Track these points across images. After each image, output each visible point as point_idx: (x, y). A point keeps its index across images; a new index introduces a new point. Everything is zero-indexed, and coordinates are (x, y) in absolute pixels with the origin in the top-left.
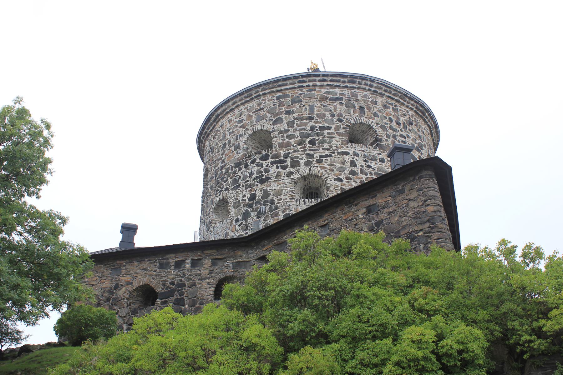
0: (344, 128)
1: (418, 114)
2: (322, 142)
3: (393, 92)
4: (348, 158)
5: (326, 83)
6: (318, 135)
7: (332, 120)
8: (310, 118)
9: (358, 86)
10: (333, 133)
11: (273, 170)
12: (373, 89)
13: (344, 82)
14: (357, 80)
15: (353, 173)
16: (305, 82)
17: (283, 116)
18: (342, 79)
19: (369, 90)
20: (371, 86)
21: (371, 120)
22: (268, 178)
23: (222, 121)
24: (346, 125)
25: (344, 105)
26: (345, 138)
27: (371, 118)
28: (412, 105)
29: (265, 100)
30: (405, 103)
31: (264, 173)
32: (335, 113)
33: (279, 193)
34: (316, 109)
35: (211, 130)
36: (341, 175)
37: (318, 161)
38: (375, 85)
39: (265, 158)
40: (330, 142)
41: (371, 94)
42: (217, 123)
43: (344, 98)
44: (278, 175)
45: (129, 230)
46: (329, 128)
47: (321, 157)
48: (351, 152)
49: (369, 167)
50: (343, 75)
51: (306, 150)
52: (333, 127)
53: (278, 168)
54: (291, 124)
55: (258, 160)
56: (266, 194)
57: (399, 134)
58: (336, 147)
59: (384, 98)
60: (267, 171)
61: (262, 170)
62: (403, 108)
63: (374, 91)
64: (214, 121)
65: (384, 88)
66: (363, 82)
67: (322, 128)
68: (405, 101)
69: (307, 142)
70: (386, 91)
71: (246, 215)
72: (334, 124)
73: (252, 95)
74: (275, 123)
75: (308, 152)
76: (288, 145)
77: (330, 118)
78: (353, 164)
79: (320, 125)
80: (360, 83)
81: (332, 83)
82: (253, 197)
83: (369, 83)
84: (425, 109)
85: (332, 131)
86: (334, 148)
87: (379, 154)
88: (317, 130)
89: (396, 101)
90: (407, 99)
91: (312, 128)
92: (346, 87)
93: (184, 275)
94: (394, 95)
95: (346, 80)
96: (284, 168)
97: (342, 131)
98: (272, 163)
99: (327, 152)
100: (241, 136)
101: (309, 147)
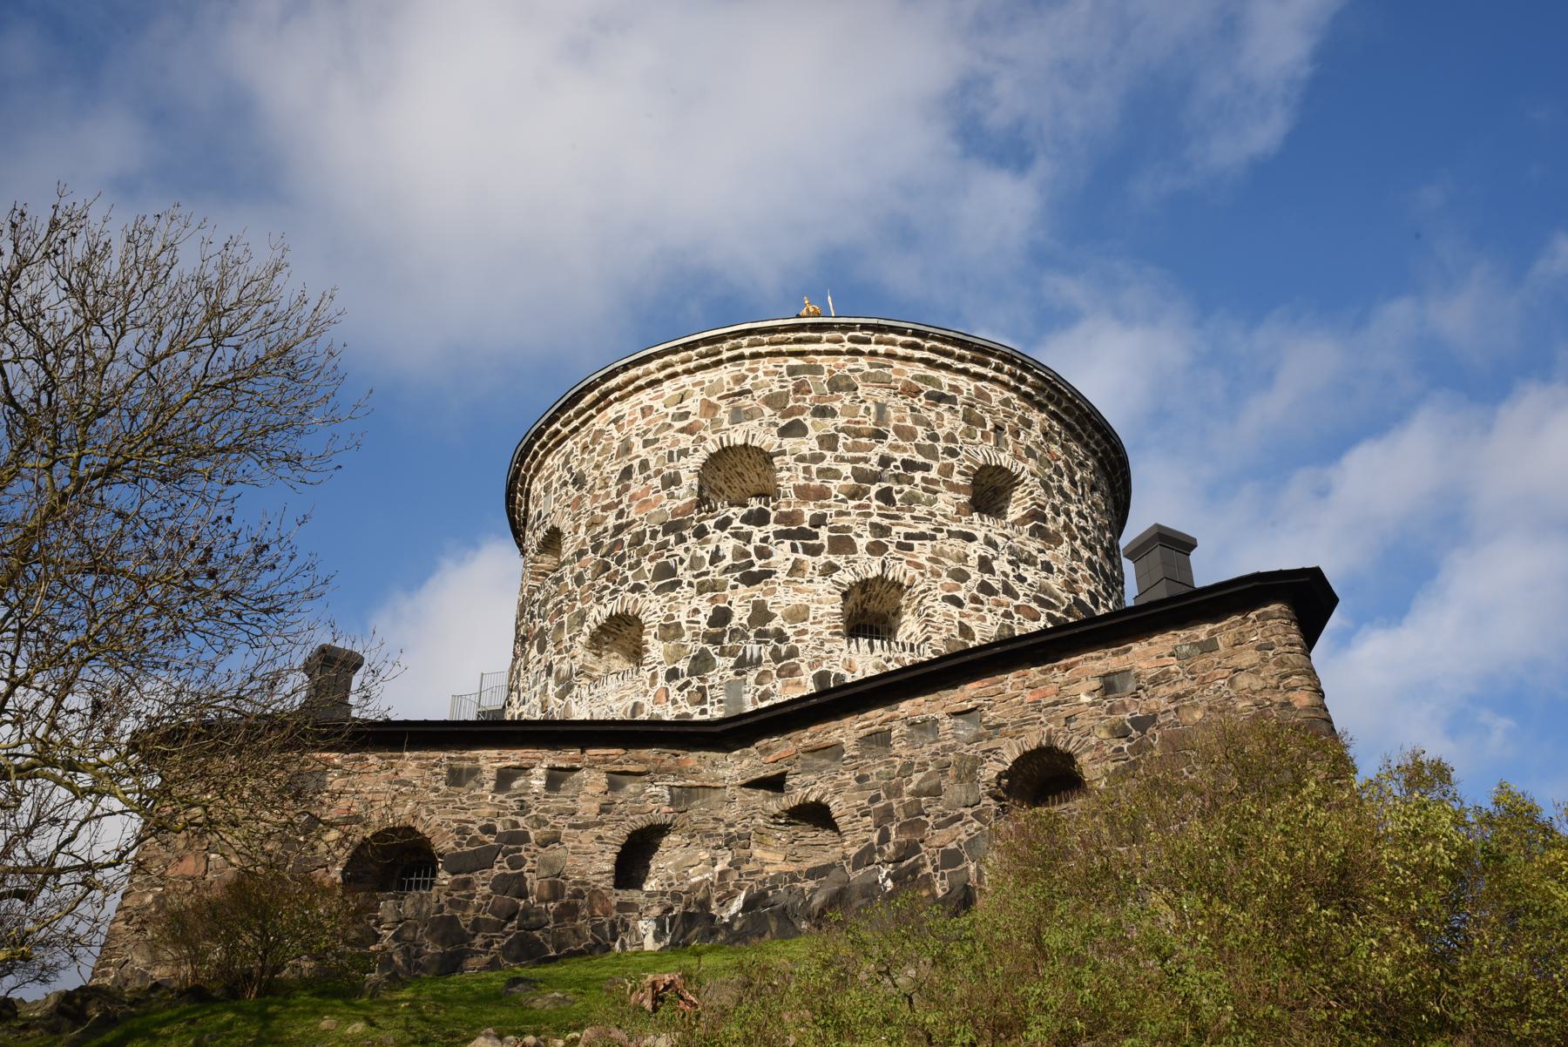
0: (960, 473)
2: (911, 499)
5: (918, 354)
6: (898, 479)
7: (934, 449)
8: (880, 435)
10: (934, 482)
11: (782, 555)
13: (961, 359)
15: (985, 588)
16: (868, 342)
17: (808, 420)
18: (957, 351)
21: (1021, 465)
22: (767, 574)
23: (616, 406)
24: (967, 467)
25: (961, 415)
26: (964, 499)
27: (1021, 459)
28: (1097, 443)
29: (756, 370)
31: (754, 558)
32: (940, 432)
33: (798, 615)
35: (576, 429)
36: (959, 588)
37: (900, 546)
38: (1030, 378)
39: (760, 518)
40: (931, 503)
42: (599, 411)
43: (960, 399)
44: (796, 568)
47: (908, 536)
48: (980, 535)
49: (1022, 579)
51: (870, 515)
52: (936, 465)
53: (794, 549)
54: (829, 442)
55: (736, 523)
56: (761, 614)
58: (945, 516)
60: (763, 553)
61: (750, 548)
64: (591, 406)
66: (1007, 367)
67: (909, 465)
69: (872, 494)
71: (701, 663)
72: (937, 459)
73: (720, 353)
74: (784, 432)
75: (876, 519)
76: (822, 494)
77: (928, 442)
78: (985, 565)
79: (906, 456)
80: (998, 369)
81: (933, 356)
82: (721, 617)
85: (933, 474)
86: (940, 518)
87: (1040, 551)
88: (897, 467)
91: (885, 461)
92: (965, 372)
93: (523, 808)
94: (1065, 410)
96: (814, 551)
97: (956, 479)
98: (779, 535)
99: (923, 527)
100: (684, 453)
101: (879, 508)
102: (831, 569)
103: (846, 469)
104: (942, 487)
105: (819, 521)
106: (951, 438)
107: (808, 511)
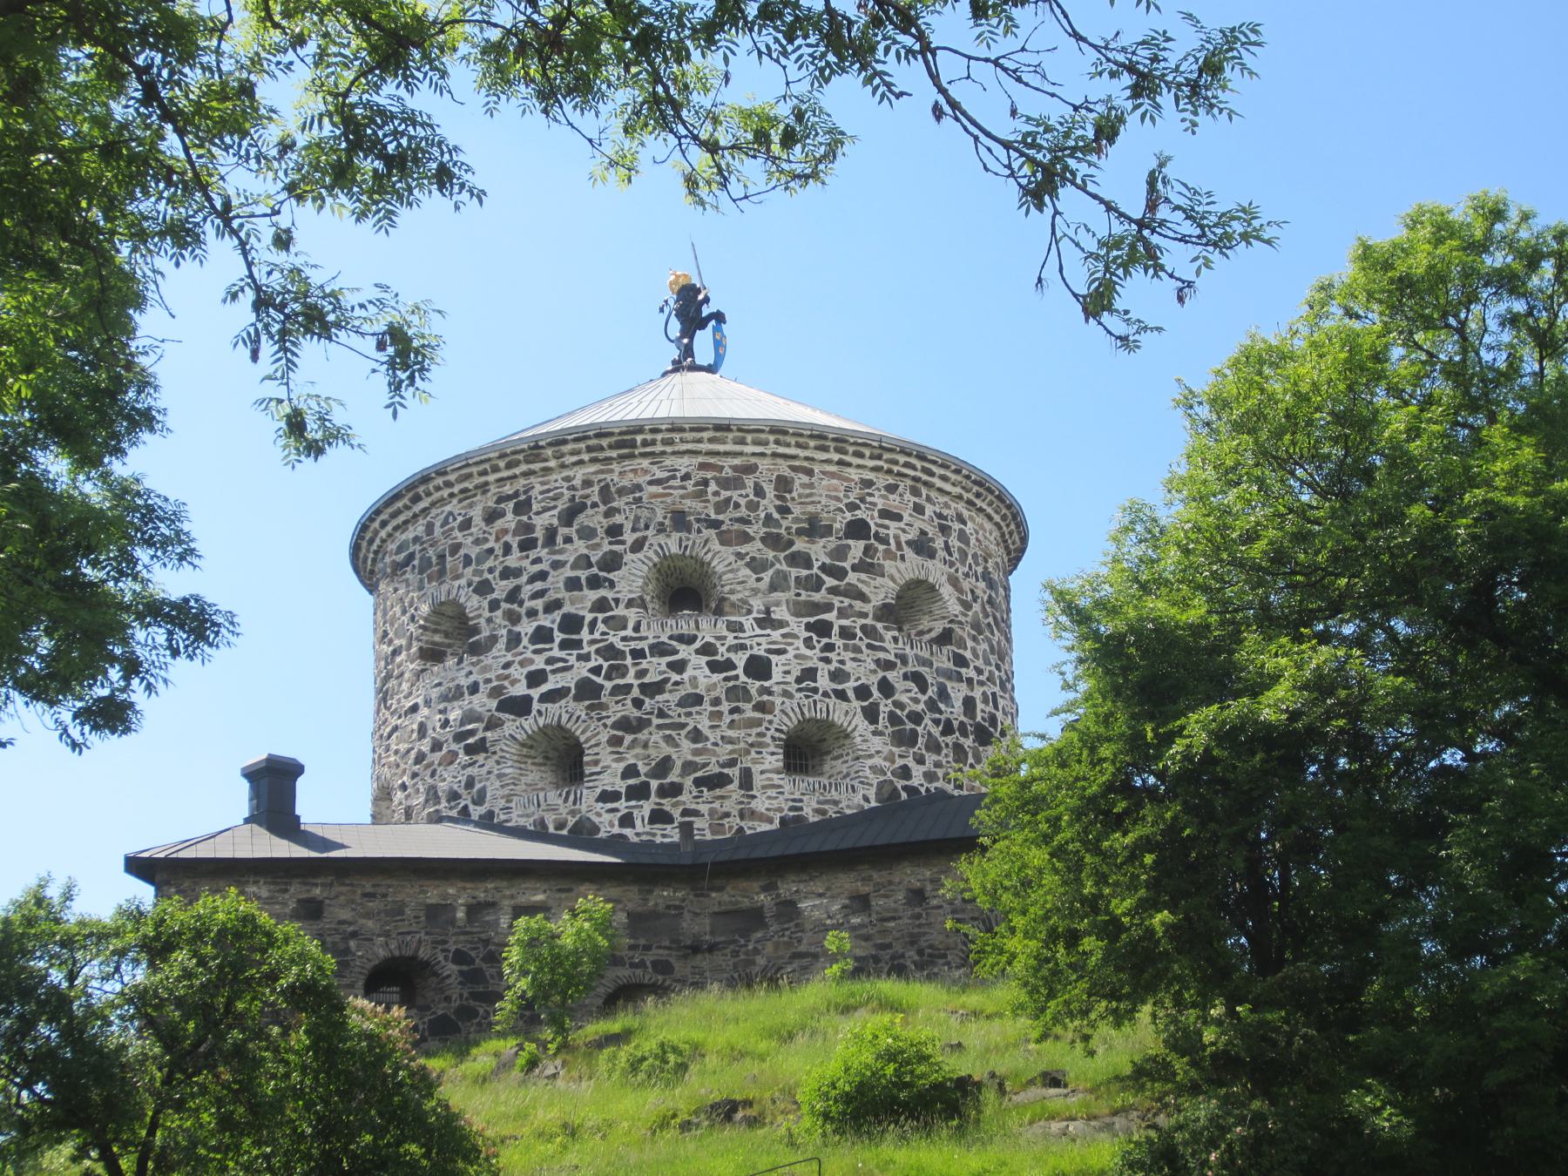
1: (609, 460)
3: (502, 464)
9: (429, 500)
12: (456, 490)
13: (407, 508)
14: (421, 490)
18: (400, 504)
19: (452, 495)
20: (448, 484)
28: (573, 453)
30: (552, 464)
38: (452, 478)
41: (460, 501)
50: (395, 497)
57: (524, 578)
59: (493, 489)
62: (554, 477)
63: (463, 491)
65: (475, 470)
68: (546, 460)
70: (484, 473)
80: (428, 494)
83: (440, 481)
84: (621, 434)
89: (526, 474)
90: (549, 452)
94: (509, 466)
95: (406, 501)
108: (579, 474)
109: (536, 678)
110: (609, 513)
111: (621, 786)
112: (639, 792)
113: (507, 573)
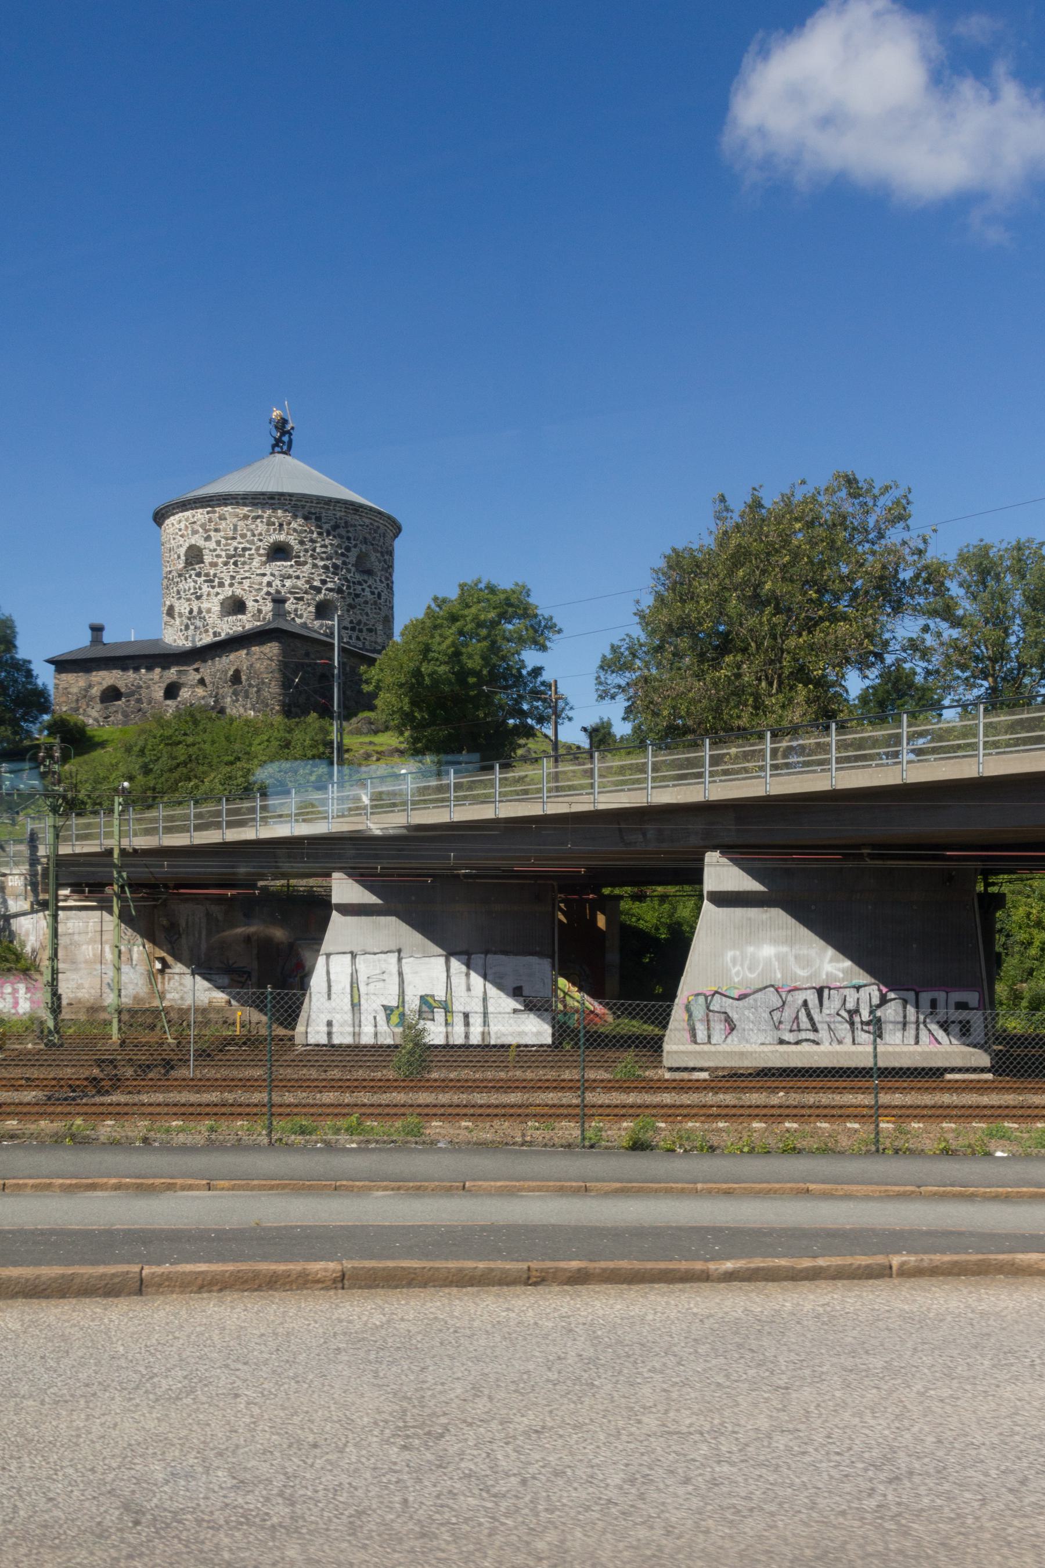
2: (244, 563)
4: (266, 579)
6: (240, 556)
8: (234, 538)
11: (205, 588)
17: (212, 534)
26: (264, 559)
33: (209, 611)
34: (239, 528)
39: (199, 575)
40: (250, 564)
44: (209, 595)
45: (97, 630)
46: (250, 549)
48: (268, 573)
56: (200, 612)
59: (307, 508)
60: (200, 589)
67: (244, 549)
71: (187, 627)
82: (191, 612)
85: (253, 552)
91: (236, 549)
93: (141, 679)
96: (213, 587)
97: (262, 551)
98: (205, 581)
99: (247, 574)
102: (218, 594)
103: (223, 554)
104: (256, 556)
105: (215, 575)
106: (260, 534)
107: (212, 572)
108: (339, 514)
109: (324, 582)
110: (348, 532)
111: (349, 626)
112: (353, 629)
113: (312, 541)
